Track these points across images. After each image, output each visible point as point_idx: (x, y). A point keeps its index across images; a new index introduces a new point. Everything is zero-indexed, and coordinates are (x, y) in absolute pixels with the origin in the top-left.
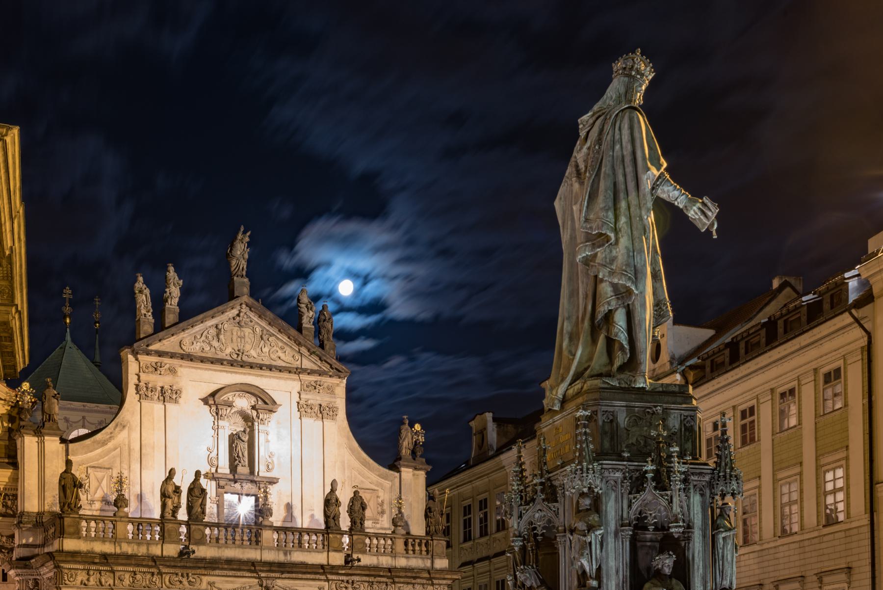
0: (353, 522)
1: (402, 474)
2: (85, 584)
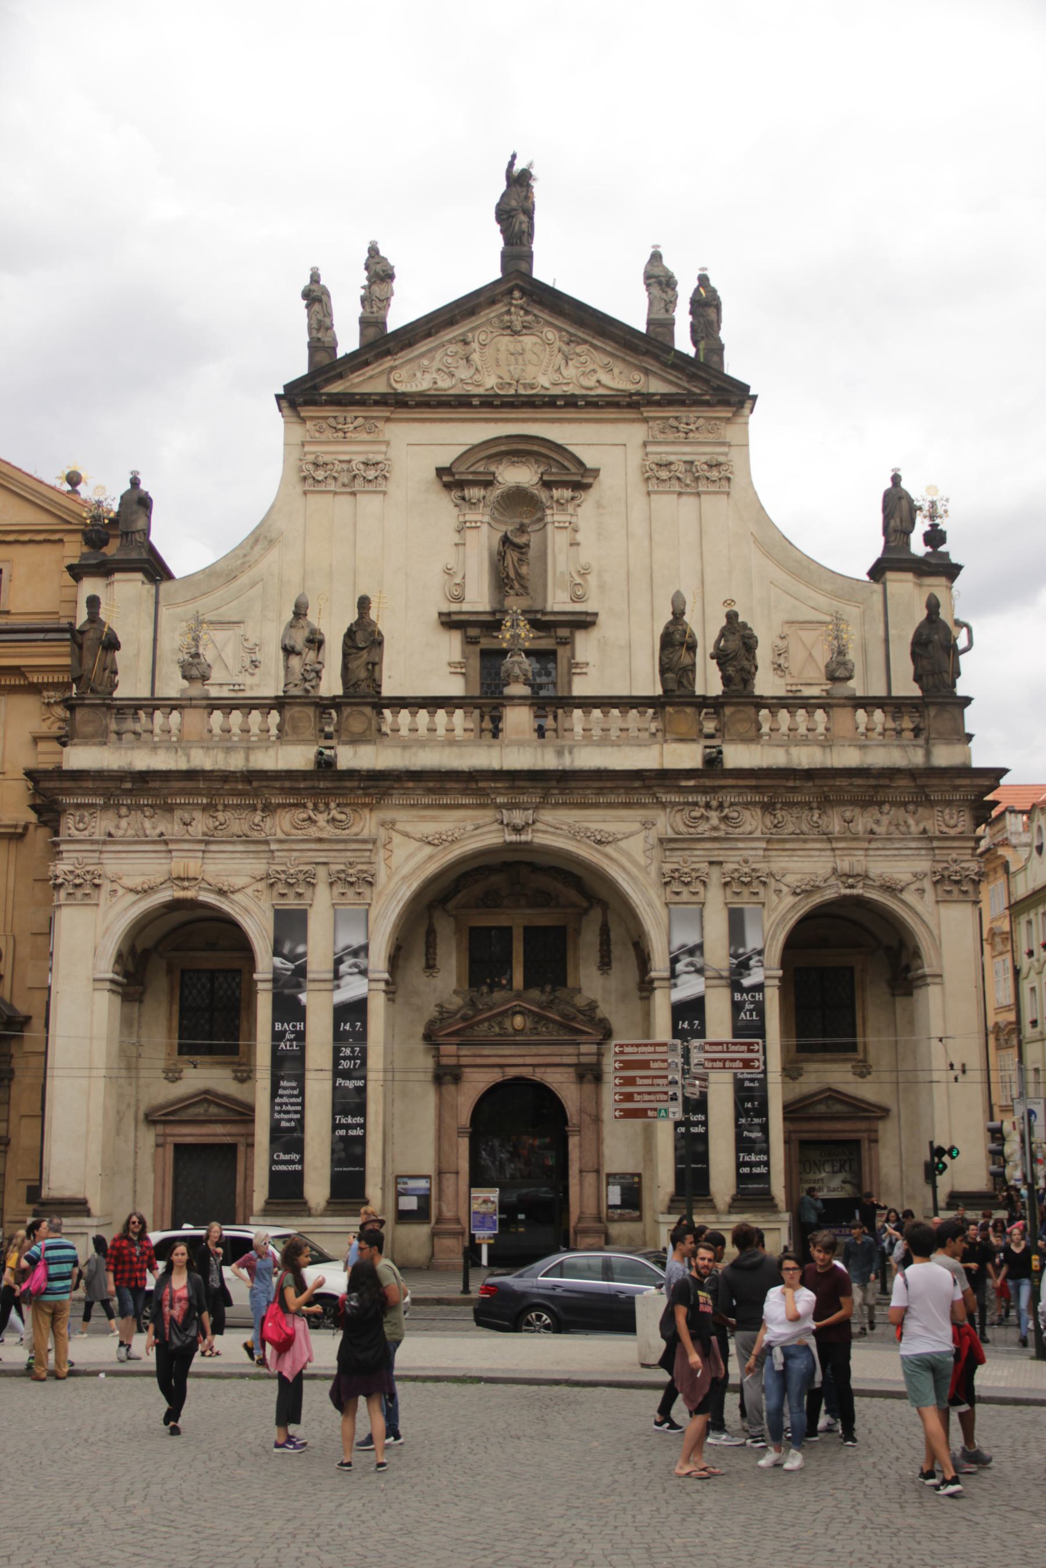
0: (726, 680)
1: (888, 584)
2: (110, 835)
